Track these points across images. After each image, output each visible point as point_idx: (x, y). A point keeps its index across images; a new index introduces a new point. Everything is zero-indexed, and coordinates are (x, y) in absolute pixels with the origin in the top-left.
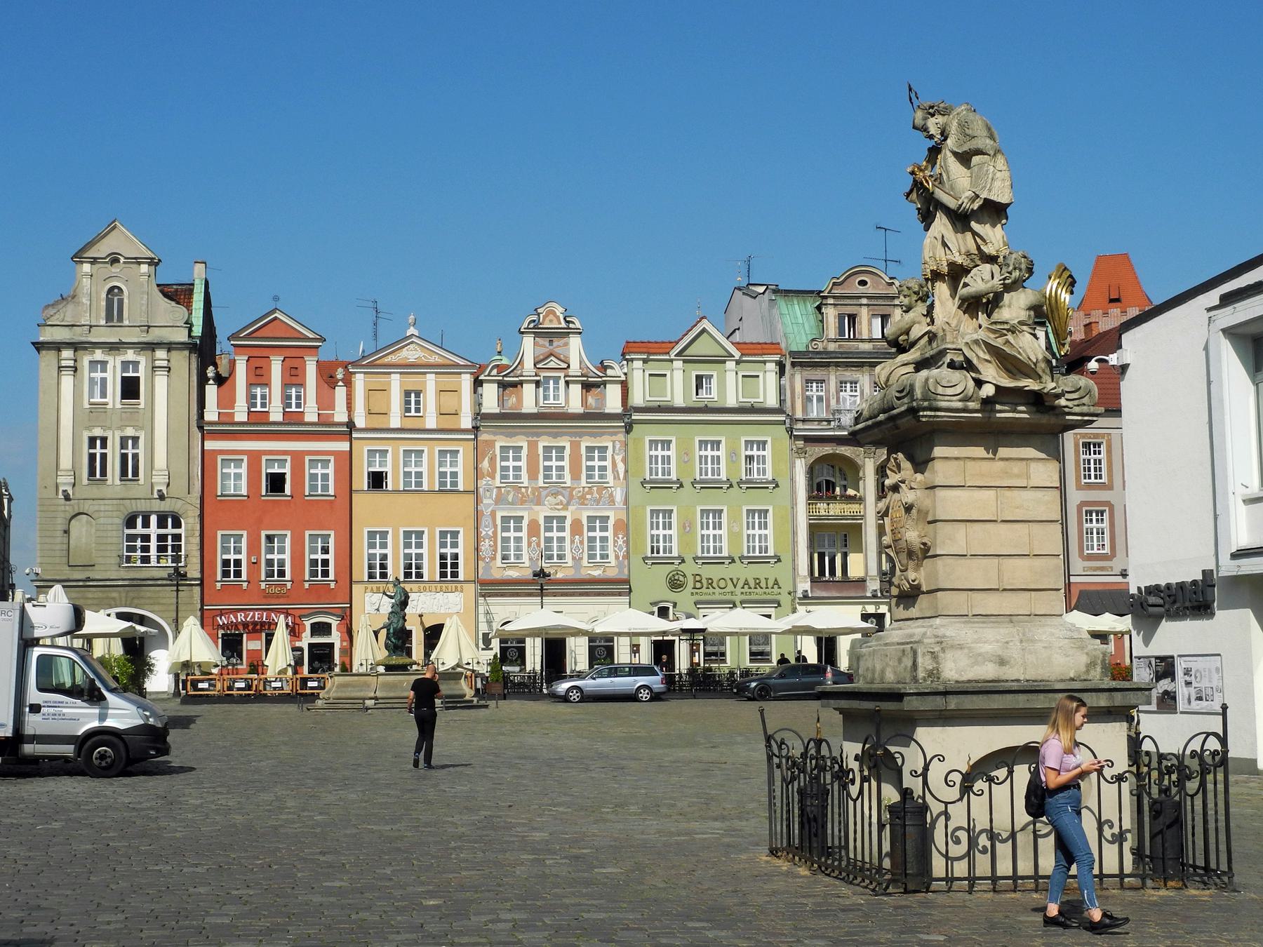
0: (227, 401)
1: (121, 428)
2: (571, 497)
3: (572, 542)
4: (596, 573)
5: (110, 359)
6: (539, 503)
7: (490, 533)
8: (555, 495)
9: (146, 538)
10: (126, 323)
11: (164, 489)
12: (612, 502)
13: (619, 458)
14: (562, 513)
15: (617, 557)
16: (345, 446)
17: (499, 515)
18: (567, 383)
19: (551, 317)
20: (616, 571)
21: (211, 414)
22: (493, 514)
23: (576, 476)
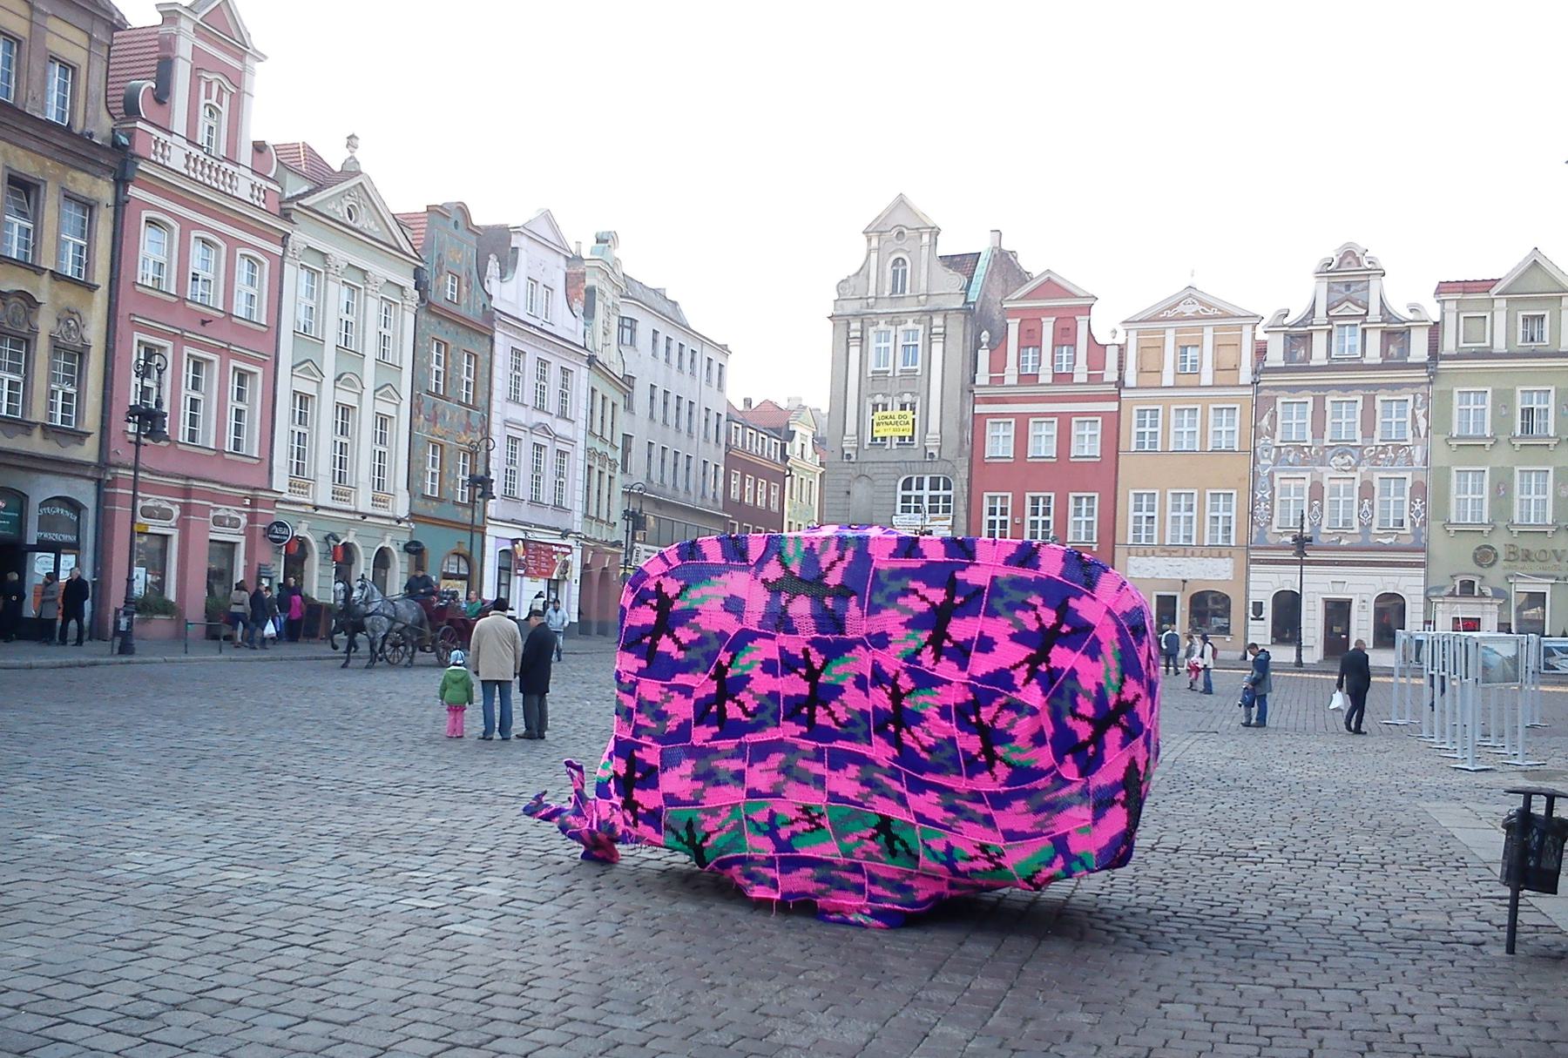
0: (998, 365)
1: (901, 394)
3: (1361, 506)
4: (1387, 541)
5: (892, 328)
8: (1342, 455)
9: (919, 499)
10: (907, 292)
11: (936, 452)
12: (1410, 460)
13: (1420, 413)
14: (1351, 475)
15: (1413, 524)
16: (1113, 406)
18: (1364, 330)
19: (1349, 259)
20: (1412, 539)
21: (983, 378)
22: (1271, 475)
23: (1368, 432)
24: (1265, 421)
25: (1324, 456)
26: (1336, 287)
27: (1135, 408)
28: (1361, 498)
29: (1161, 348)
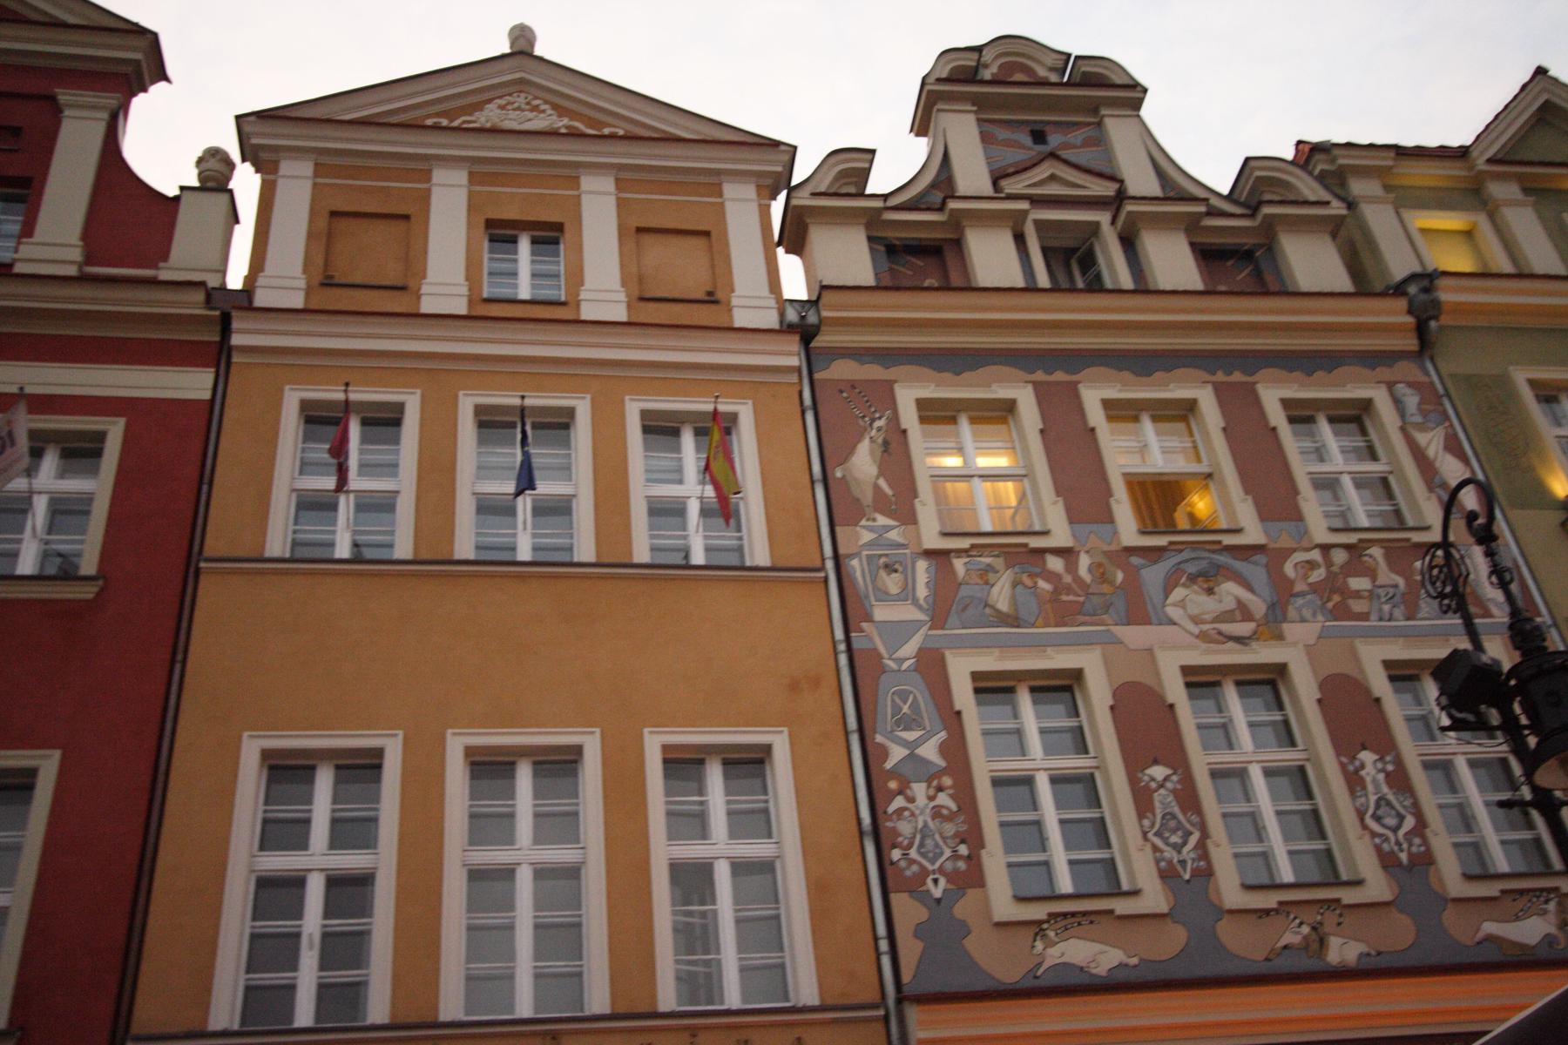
2: (1282, 596)
3: (1354, 781)
6: (1138, 613)
7: (930, 751)
8: (1207, 579)
13: (1432, 441)
17: (960, 670)
18: (1129, 242)
22: (932, 666)
24: (863, 463)
25: (1133, 589)
26: (1002, 134)
27: (292, 400)
28: (1346, 745)
29: (407, 219)
